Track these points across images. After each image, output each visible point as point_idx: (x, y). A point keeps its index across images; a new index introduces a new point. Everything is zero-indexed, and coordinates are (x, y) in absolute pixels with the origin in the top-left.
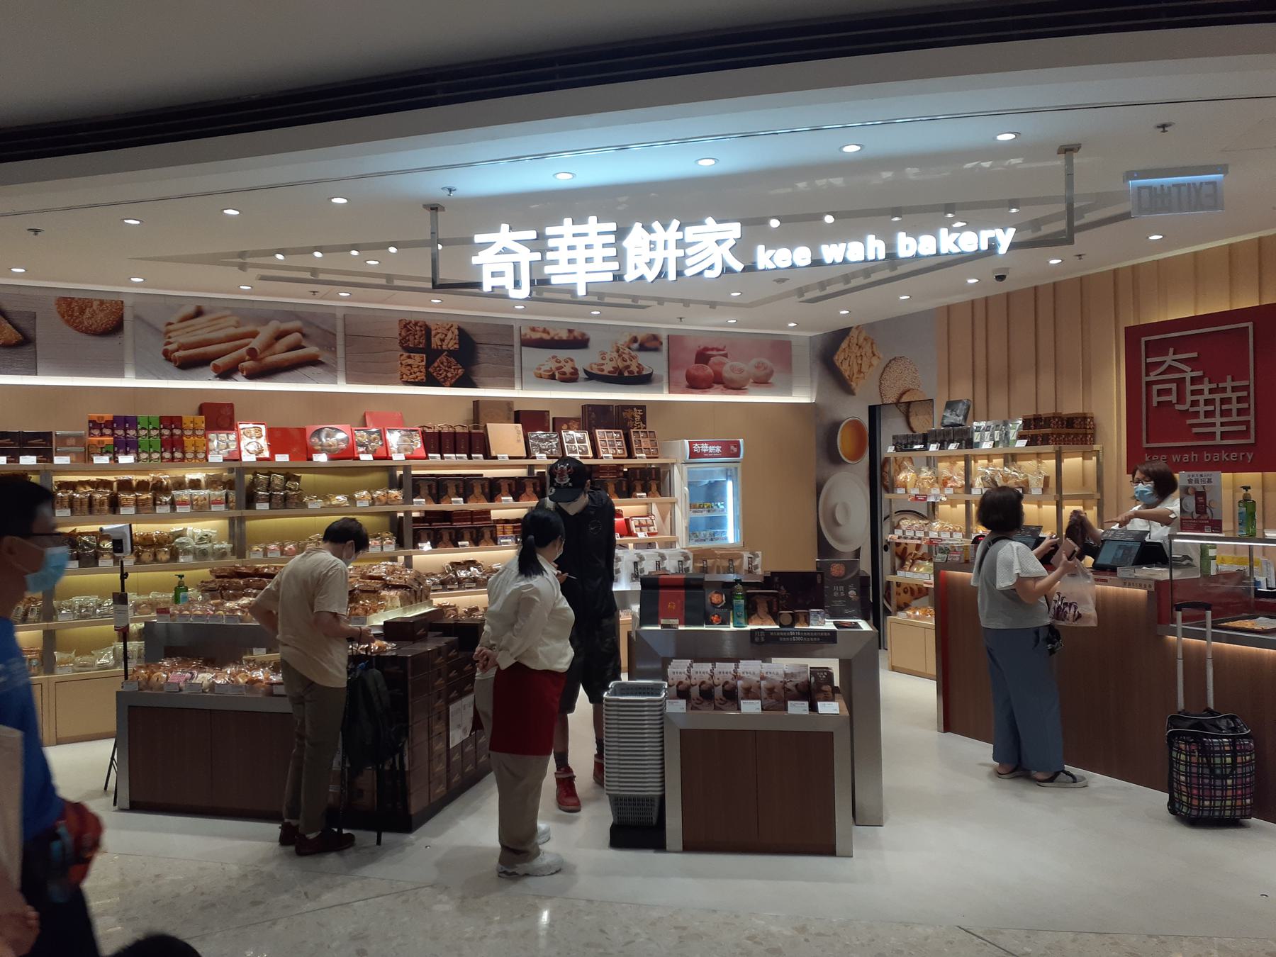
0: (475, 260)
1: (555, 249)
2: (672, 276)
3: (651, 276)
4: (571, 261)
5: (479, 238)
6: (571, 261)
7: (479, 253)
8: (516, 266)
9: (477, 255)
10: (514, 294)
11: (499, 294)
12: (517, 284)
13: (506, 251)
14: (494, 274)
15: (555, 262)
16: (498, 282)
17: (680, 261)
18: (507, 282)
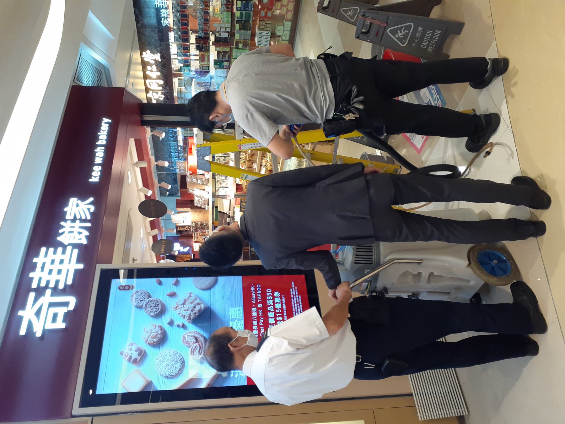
0: (39, 334)
1: (48, 282)
2: (89, 225)
3: (87, 233)
4: (59, 272)
5: (23, 331)
6: (59, 272)
7: (35, 331)
8: (51, 305)
9: (36, 332)
10: (71, 307)
11: (68, 316)
12: (66, 304)
13: (38, 313)
14: (54, 320)
15: (57, 282)
16: (60, 318)
17: (82, 221)
18: (62, 311)
